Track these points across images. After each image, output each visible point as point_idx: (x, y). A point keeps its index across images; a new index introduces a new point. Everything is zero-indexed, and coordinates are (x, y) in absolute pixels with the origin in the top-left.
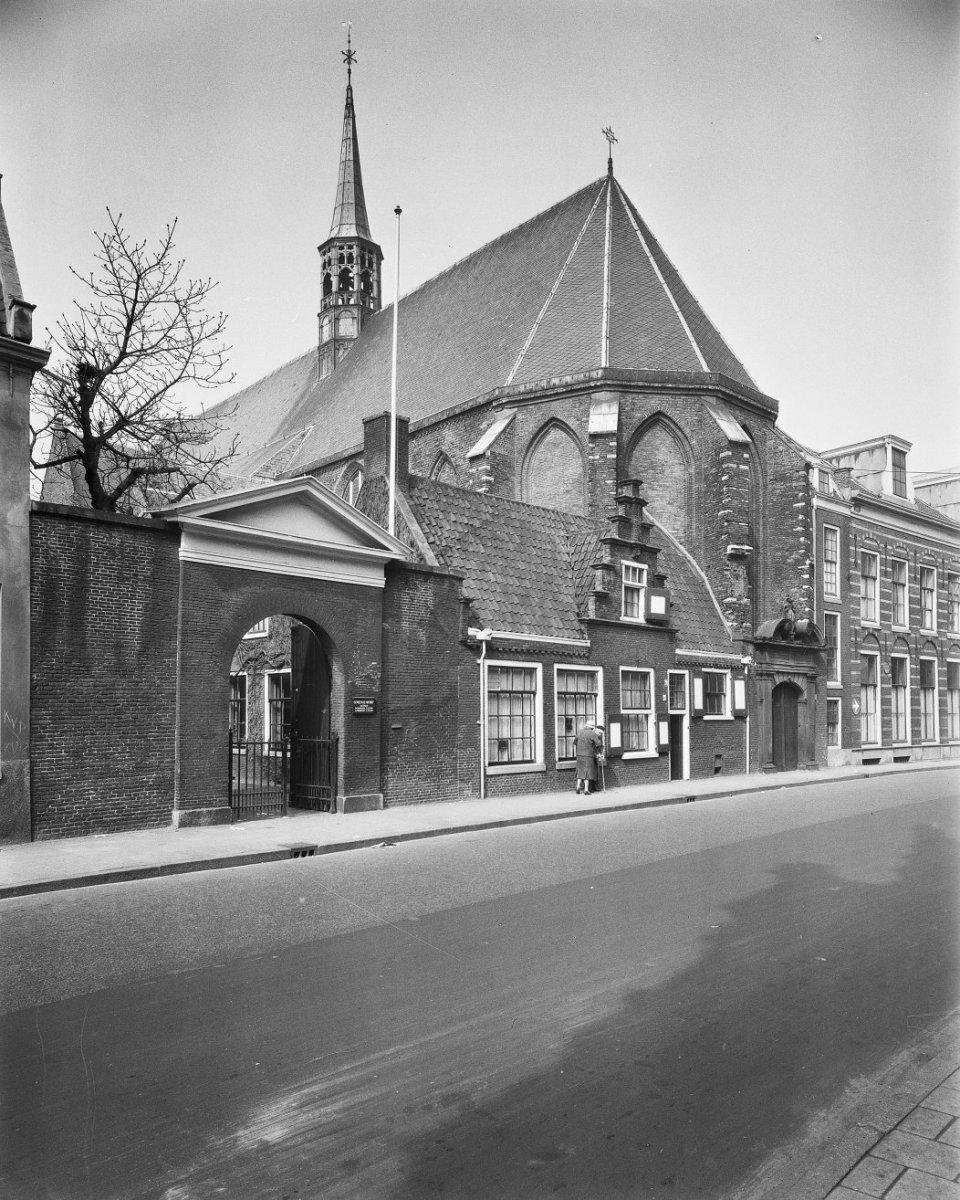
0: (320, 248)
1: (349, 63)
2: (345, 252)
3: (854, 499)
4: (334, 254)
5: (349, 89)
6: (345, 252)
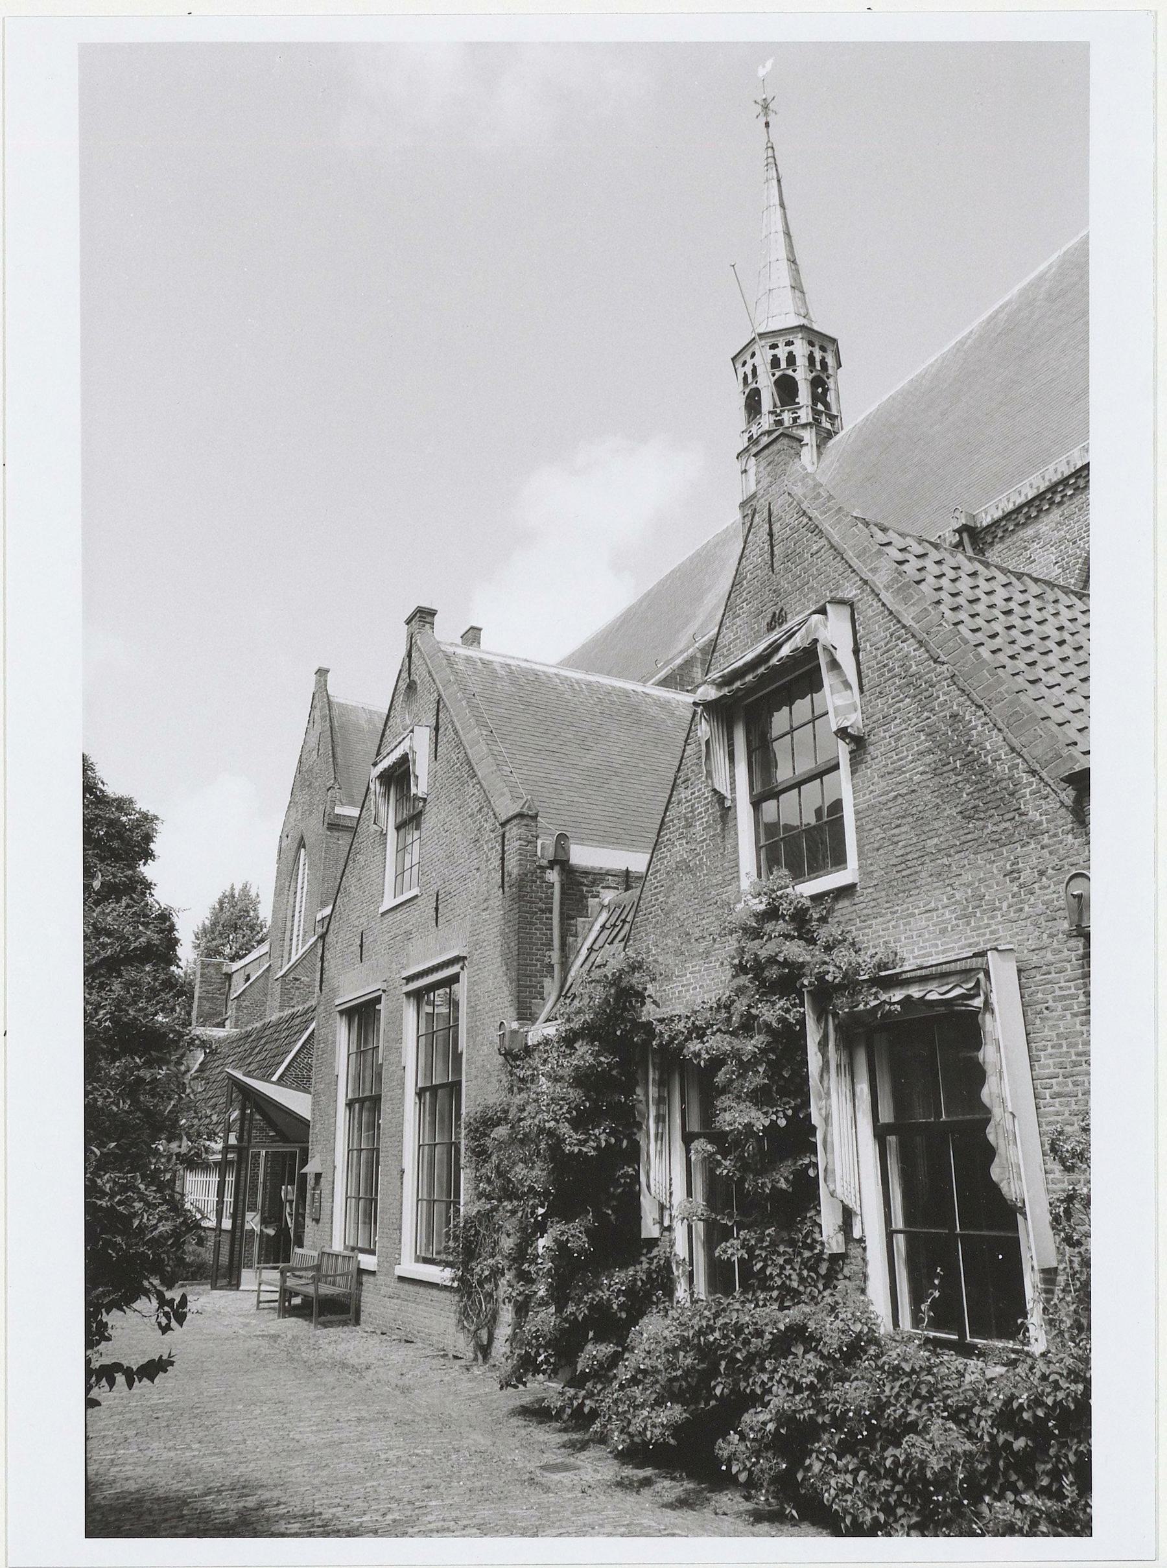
1: (766, 114)
2: (782, 353)
6: (782, 353)
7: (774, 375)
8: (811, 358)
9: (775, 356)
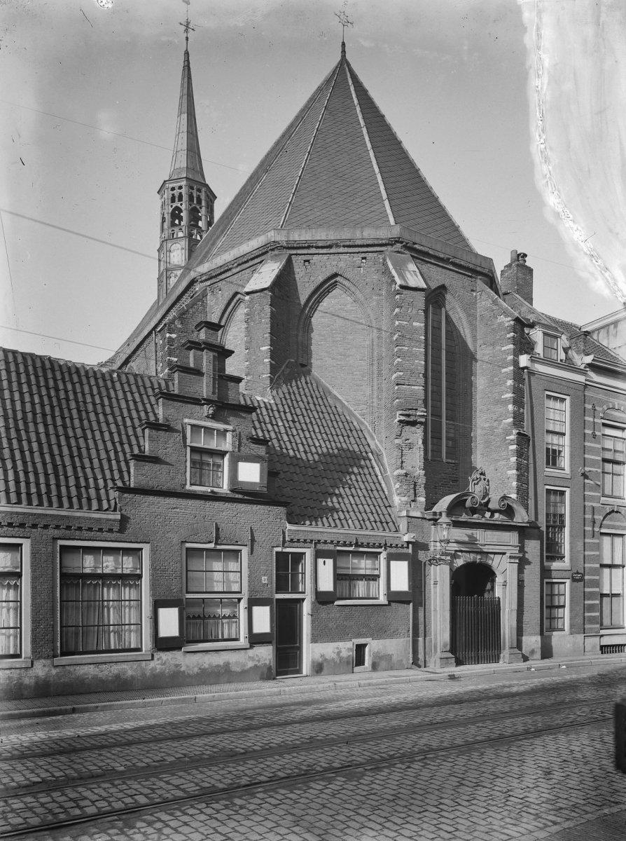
0: (158, 192)
2: (176, 192)
3: (590, 365)
4: (168, 194)
5: (187, 53)
7: (172, 206)
8: (191, 197)
9: (173, 195)
